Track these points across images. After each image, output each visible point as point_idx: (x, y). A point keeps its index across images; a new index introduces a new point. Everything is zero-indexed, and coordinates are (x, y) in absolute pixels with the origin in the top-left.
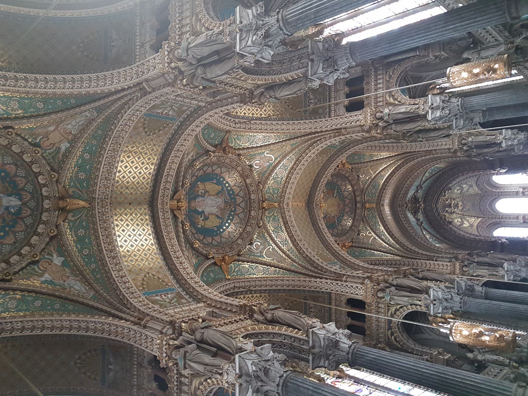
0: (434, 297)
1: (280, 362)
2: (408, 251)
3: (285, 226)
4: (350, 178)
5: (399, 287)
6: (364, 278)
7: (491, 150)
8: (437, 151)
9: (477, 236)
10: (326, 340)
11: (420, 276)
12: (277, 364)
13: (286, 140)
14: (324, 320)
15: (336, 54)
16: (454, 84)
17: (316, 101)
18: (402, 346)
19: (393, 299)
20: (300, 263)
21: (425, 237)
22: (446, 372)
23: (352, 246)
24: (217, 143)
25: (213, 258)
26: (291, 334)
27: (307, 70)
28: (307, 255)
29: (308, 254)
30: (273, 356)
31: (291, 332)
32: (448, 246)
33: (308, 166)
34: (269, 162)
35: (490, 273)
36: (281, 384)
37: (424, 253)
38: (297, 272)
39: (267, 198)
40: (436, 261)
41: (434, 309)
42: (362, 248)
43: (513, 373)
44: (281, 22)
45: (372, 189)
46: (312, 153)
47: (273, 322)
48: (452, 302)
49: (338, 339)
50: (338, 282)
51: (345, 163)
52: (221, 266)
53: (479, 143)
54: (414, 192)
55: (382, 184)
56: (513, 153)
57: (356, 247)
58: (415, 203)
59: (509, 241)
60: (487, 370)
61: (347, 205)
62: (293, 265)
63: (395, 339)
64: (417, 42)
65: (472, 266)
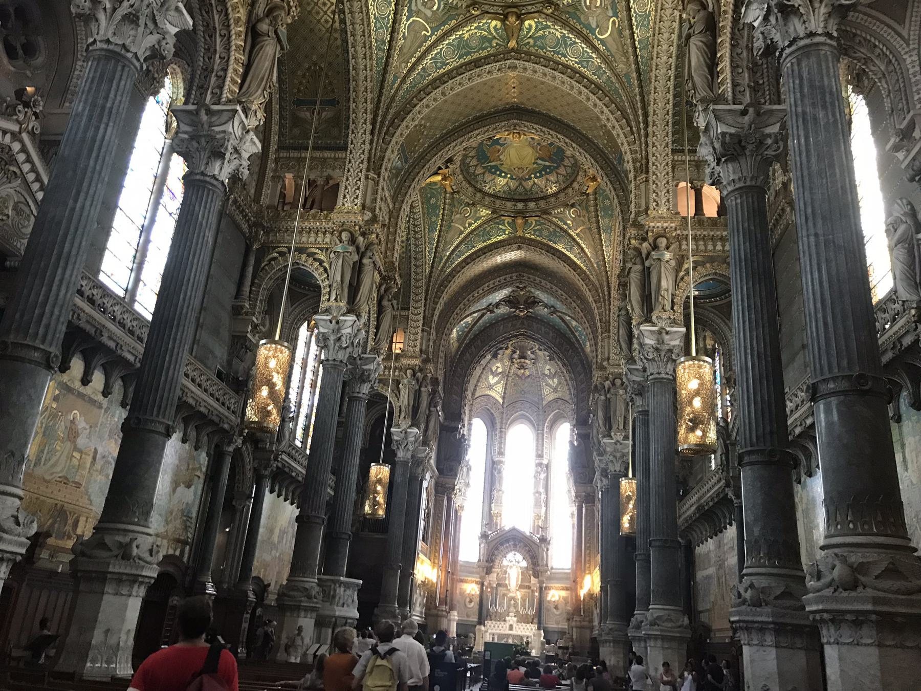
0: (342, 321)
1: (157, 46)
2: (439, 287)
3: (470, 63)
5: (358, 269)
6: (373, 210)
7: (601, 423)
8: (606, 340)
9: (473, 394)
10: (222, 135)
11: (385, 303)
12: (152, 40)
13: (637, 63)
14: (264, 133)
15: (749, 160)
16: (680, 368)
18: (263, 268)
19: (338, 257)
20: (401, 93)
21: (468, 316)
22: (181, 328)
23: (446, 192)
26: (230, 70)
27: (726, 102)
28: (415, 106)
29: (417, 108)
30: (167, 32)
31: (235, 70)
32: (453, 349)
33: (587, 109)
34: (598, 26)
35: (403, 409)
36: (111, 47)
37: (437, 313)
38: (382, 87)
39: (527, 23)
40: (423, 330)
41: (324, 320)
42: (444, 209)
43: (232, 427)
44: (807, 41)
45: (548, 229)
46: (608, 117)
47: (254, 35)
48: (336, 348)
49: (227, 156)
50: (365, 163)
53: (612, 403)
54: (546, 300)
55: (558, 247)
56: (595, 453)
57: (445, 198)
59: (460, 439)
60: (233, 394)
61: (521, 184)
62: (395, 78)
63: (274, 259)
64: (738, 306)
65: (414, 382)
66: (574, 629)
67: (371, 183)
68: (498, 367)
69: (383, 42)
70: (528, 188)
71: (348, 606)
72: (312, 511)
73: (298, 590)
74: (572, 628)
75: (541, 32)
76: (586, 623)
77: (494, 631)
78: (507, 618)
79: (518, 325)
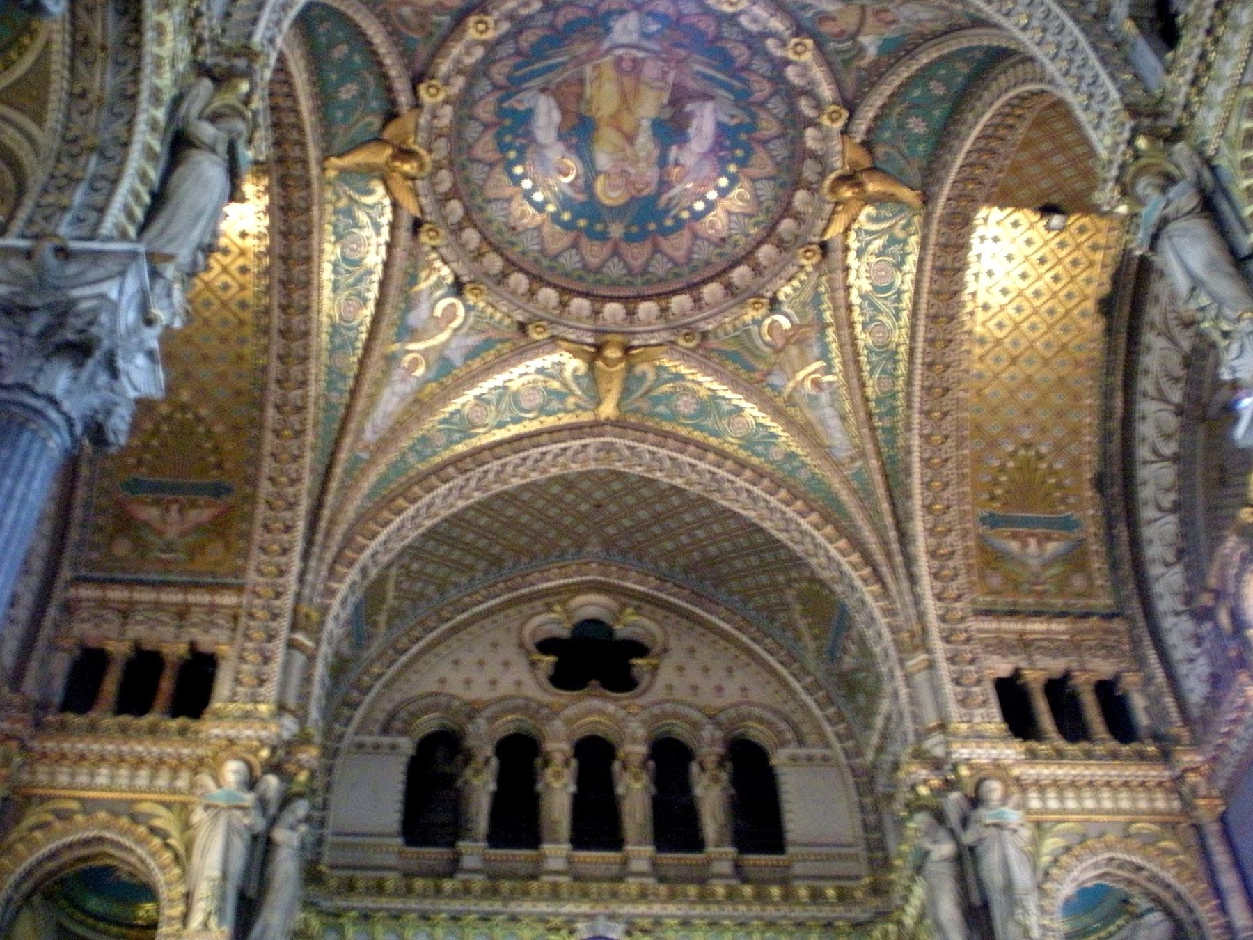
17: (1034, 563)
24: (880, 151)
25: (417, 105)
52: (378, 140)
67: (299, 658)
69: (344, 377)
75: (667, 388)
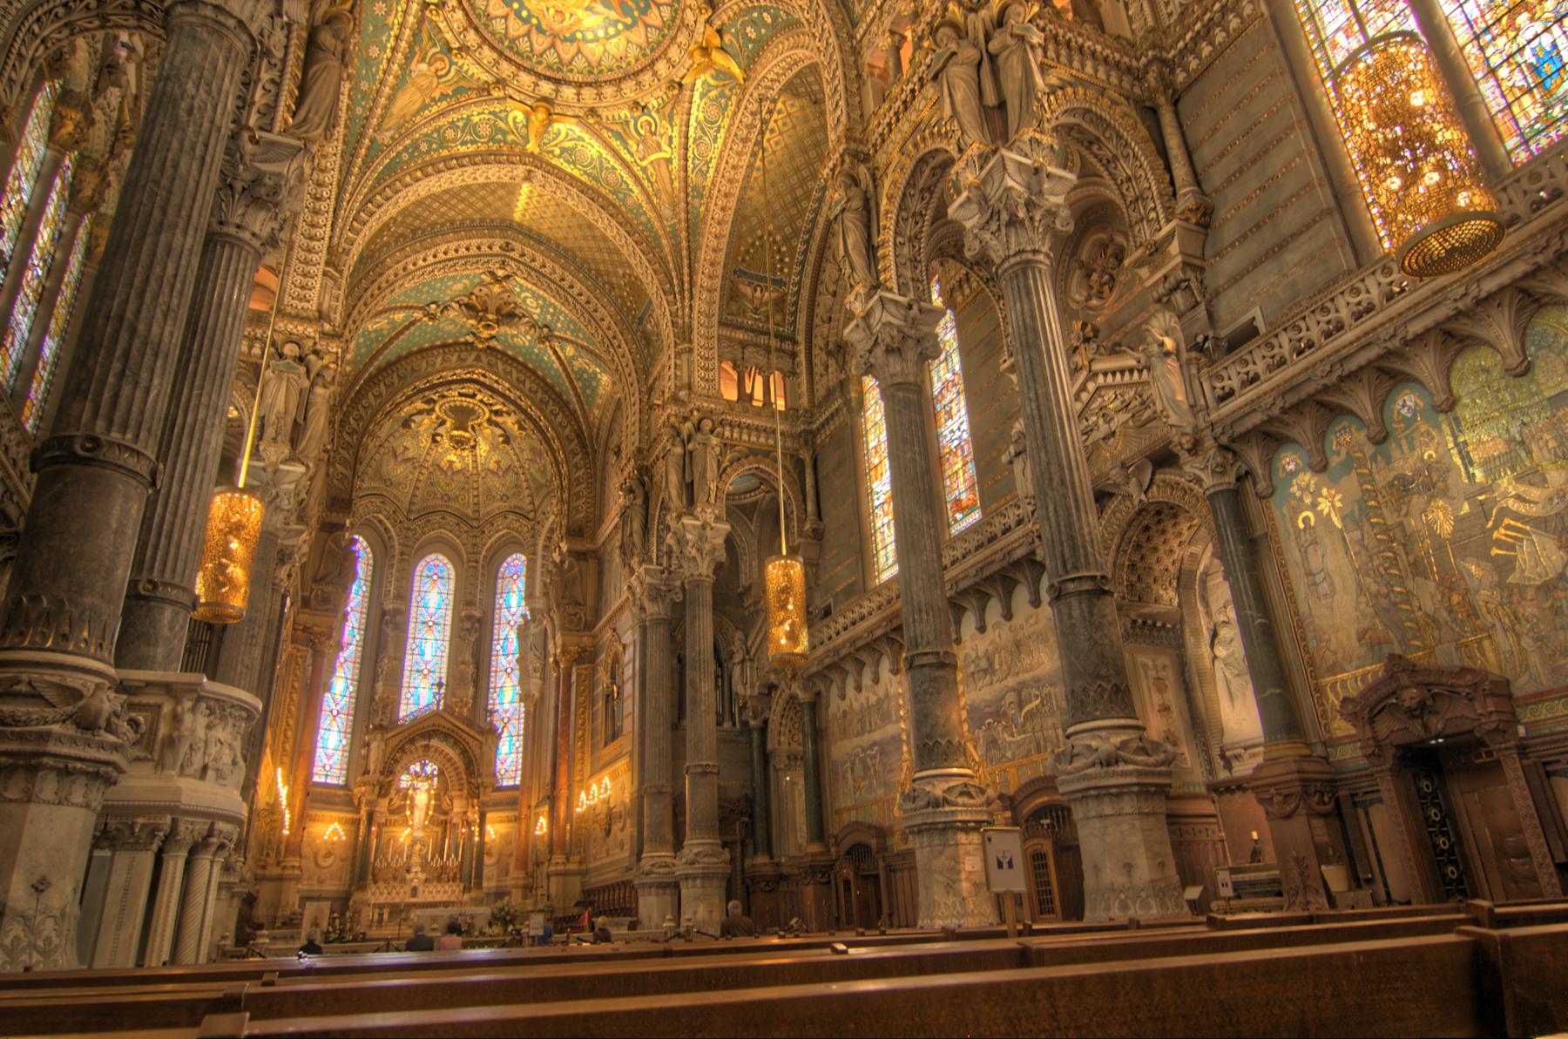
4: (647, 77)
8: (685, 357)
40: (325, 274)
51: (709, 55)
57: (405, 13)
58: (498, 311)
61: (553, 46)
66: (553, 880)
68: (406, 449)
70: (566, 57)
71: (220, 775)
72: (109, 427)
73: (34, 696)
74: (548, 876)
76: (572, 867)
77: (382, 900)
78: (409, 876)
79: (470, 361)
